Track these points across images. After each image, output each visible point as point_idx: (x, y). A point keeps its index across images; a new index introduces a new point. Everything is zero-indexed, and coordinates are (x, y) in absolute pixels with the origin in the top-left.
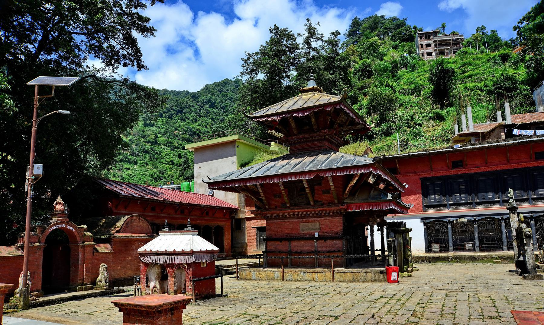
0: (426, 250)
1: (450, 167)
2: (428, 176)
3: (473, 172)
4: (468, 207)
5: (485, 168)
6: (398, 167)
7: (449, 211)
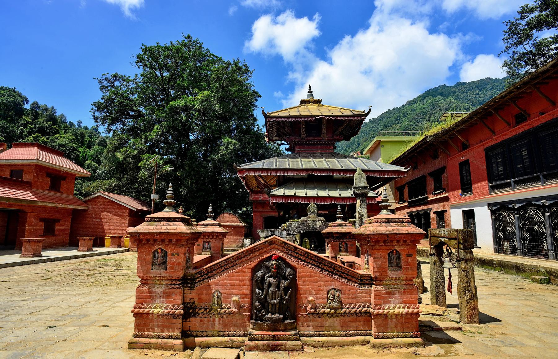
2: (490, 144)
3: (535, 125)
4: (536, 184)
5: (550, 115)
6: (462, 139)
7: (513, 192)
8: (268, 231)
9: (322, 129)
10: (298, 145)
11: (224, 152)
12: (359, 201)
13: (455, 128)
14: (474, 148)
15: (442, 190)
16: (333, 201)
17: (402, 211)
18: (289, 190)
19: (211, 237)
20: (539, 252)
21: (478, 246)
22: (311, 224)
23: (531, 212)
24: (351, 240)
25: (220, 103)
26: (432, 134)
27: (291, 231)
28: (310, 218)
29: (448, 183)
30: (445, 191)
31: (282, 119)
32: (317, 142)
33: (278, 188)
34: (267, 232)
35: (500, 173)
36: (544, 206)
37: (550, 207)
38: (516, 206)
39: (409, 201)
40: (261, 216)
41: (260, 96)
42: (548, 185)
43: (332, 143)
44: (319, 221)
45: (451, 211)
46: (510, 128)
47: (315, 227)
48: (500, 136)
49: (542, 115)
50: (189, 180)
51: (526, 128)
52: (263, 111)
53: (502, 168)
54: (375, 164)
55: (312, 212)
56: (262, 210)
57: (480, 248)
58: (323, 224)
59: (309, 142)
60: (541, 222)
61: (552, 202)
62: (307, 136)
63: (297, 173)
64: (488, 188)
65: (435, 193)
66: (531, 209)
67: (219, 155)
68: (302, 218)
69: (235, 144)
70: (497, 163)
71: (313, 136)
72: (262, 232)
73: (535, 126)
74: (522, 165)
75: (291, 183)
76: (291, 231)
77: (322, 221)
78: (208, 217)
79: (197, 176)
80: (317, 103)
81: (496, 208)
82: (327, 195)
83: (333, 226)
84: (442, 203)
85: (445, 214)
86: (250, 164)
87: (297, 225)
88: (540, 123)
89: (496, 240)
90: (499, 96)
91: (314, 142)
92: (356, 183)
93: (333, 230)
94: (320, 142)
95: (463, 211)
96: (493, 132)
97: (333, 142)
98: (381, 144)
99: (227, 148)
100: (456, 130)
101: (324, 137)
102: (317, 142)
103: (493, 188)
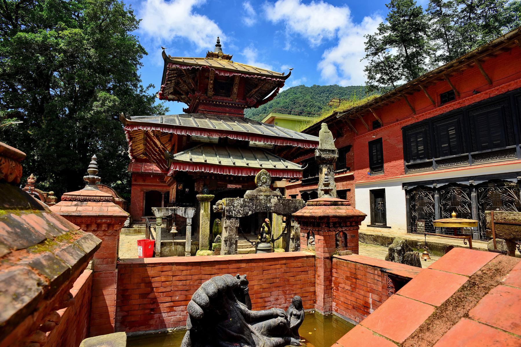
0: (408, 229)
1: (437, 104)
2: (409, 123)
3: (467, 104)
5: (487, 93)
7: (434, 172)
8: (167, 209)
9: (232, 89)
10: (204, 104)
11: (99, 109)
12: (326, 169)
13: (373, 104)
14: (389, 127)
15: (345, 169)
16: (253, 172)
17: (294, 189)
18: (198, 156)
19: (94, 227)
20: (430, 230)
21: (388, 225)
22: (263, 201)
23: (455, 192)
24: (352, 228)
25: (96, 49)
26: (342, 111)
27: (234, 212)
28: (261, 191)
29: (354, 162)
30: (349, 169)
31: (188, 67)
32: (226, 103)
33: (183, 152)
34: (165, 210)
35: (420, 152)
36: (435, 189)
37: (477, 187)
38: (436, 186)
39: (303, 179)
40: (142, 190)
41: (146, 54)
42: (477, 165)
43: (243, 106)
44: (274, 196)
45: (356, 189)
46: (435, 107)
47: (268, 205)
48: (423, 115)
49: (476, 94)
50: (45, 142)
51: (455, 107)
52: (164, 53)
53: (423, 147)
54: (294, 134)
55: (264, 183)
56: (143, 183)
57: (390, 227)
58: (279, 202)
59: (216, 102)
60: (465, 203)
61: (481, 182)
62: (214, 95)
63: (208, 134)
64: (404, 168)
65: (337, 171)
66: (454, 189)
67: (93, 112)
68: (248, 192)
69: (114, 101)
70: (417, 142)
71: (221, 96)
72: (159, 211)
73: (467, 105)
74: (447, 145)
75: (199, 147)
76: (234, 212)
77: (279, 197)
78: (87, 183)
79: (58, 137)
80: (227, 59)
81: (412, 187)
82: (245, 165)
83: (325, 205)
84: (345, 182)
85: (348, 193)
86: (144, 118)
87: (242, 203)
88: (474, 102)
89: (410, 221)
90: (437, 70)
91: (222, 103)
92: (321, 144)
93: (328, 211)
94: (229, 104)
95: (370, 190)
96: (414, 110)
97: (244, 106)
98: (275, 121)
99: (103, 105)
100: (372, 107)
101: (235, 98)
102: (226, 103)
103: (409, 167)
